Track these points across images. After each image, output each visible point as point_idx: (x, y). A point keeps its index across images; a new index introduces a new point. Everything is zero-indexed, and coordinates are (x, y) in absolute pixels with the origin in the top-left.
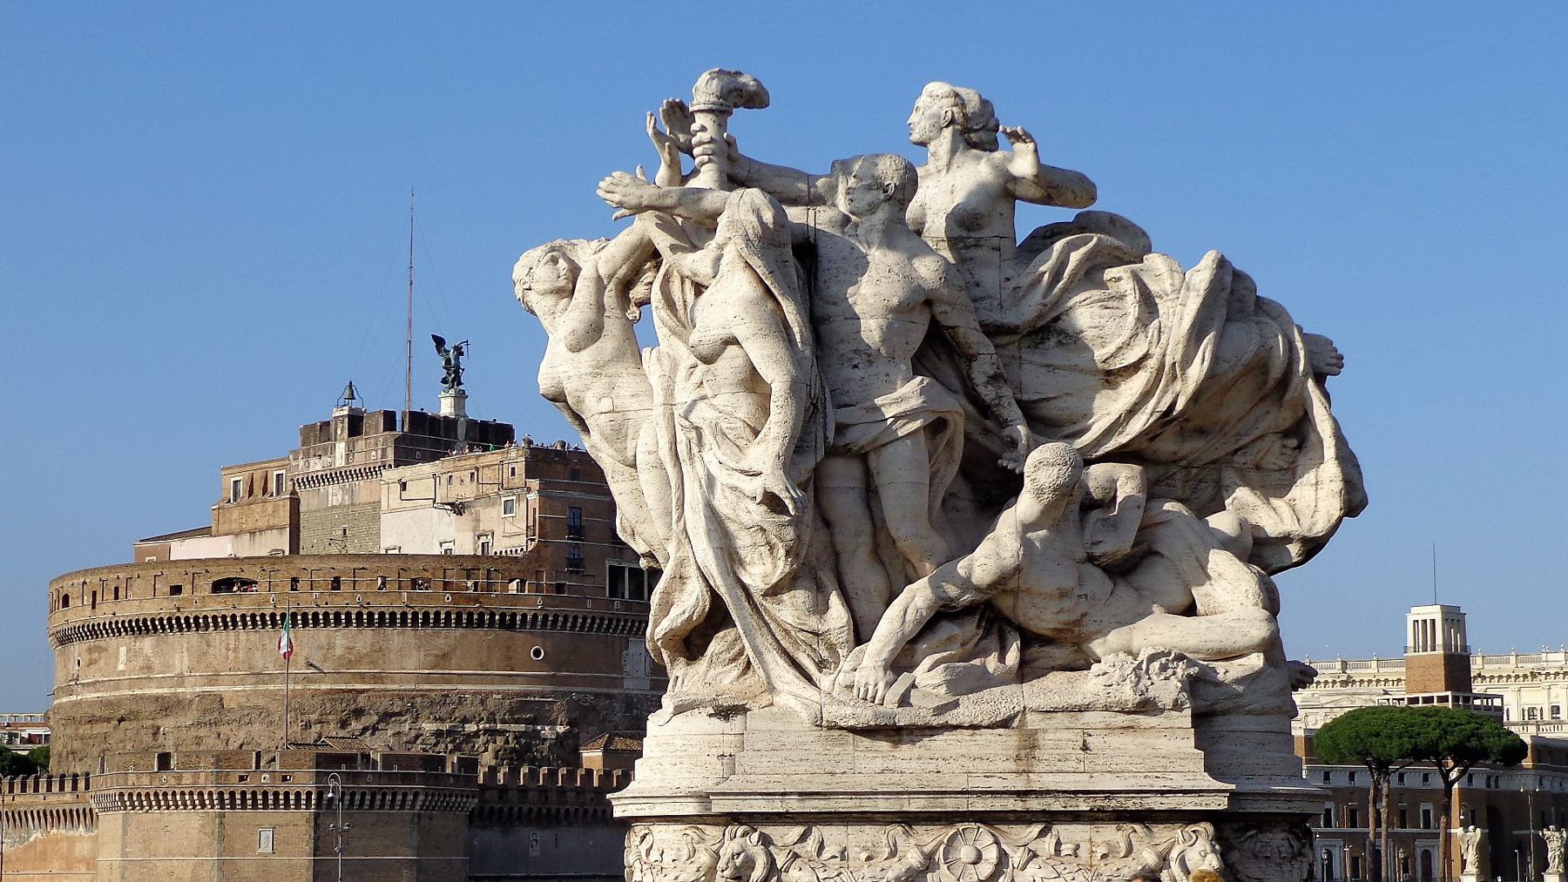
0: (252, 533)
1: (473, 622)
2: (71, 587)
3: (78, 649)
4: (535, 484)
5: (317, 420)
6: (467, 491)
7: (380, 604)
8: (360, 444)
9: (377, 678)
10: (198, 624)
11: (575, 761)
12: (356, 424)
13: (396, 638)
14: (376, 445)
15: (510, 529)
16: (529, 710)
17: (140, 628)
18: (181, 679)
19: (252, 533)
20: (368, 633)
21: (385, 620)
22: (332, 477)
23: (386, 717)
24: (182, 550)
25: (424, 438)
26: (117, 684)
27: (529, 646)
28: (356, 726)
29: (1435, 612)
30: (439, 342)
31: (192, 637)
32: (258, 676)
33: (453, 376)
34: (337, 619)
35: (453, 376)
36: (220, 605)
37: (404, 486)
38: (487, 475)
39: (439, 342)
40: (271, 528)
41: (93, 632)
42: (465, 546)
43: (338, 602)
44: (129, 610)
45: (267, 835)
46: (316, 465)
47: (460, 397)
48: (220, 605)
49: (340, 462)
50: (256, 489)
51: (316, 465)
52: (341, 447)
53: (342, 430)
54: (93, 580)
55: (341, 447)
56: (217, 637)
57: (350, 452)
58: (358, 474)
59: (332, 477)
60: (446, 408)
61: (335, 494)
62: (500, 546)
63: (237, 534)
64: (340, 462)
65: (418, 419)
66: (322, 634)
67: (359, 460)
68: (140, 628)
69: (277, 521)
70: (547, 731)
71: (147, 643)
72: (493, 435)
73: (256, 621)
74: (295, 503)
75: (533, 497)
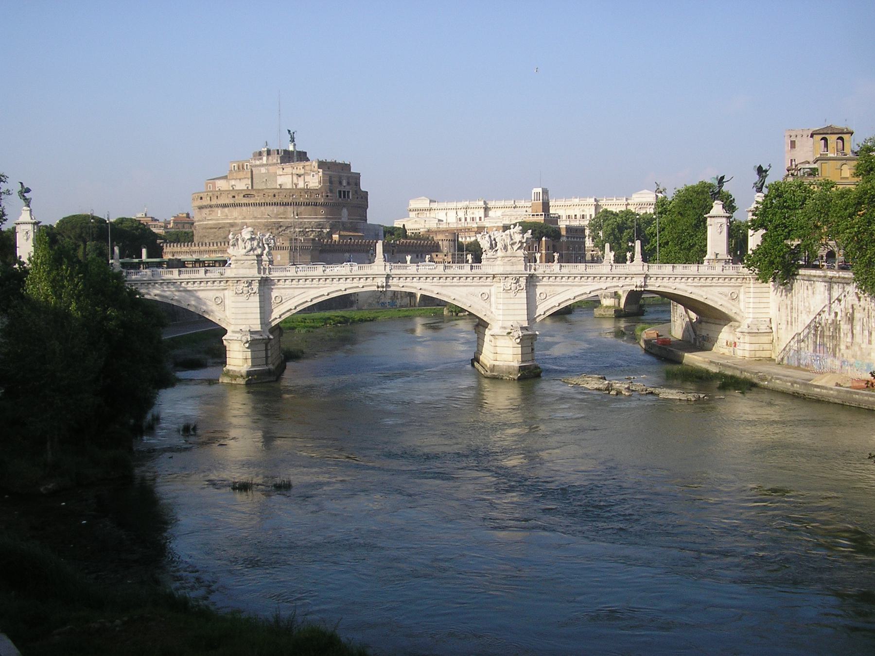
1: (308, 204)
2: (202, 195)
3: (207, 211)
4: (321, 170)
5: (258, 150)
6: (302, 171)
7: (285, 201)
8: (270, 158)
9: (285, 218)
10: (240, 205)
11: (331, 238)
12: (269, 153)
13: (290, 209)
14: (275, 159)
16: (320, 226)
17: (225, 206)
18: (236, 219)
21: (287, 204)
22: (263, 165)
23: (287, 227)
24: (222, 185)
25: (287, 157)
26: (217, 220)
27: (322, 211)
28: (280, 230)
29: (540, 190)
31: (238, 208)
32: (255, 218)
33: (293, 140)
34: (276, 204)
35: (293, 140)
36: (246, 201)
38: (307, 168)
41: (211, 206)
42: (301, 185)
43: (275, 200)
44: (221, 201)
45: (279, 256)
46: (258, 162)
47: (295, 145)
48: (246, 201)
49: (265, 162)
50: (241, 168)
51: (258, 162)
52: (265, 158)
53: (265, 154)
54: (210, 194)
55: (265, 158)
56: (244, 208)
57: (268, 159)
58: (270, 165)
59: (263, 165)
60: (291, 148)
61: (263, 170)
63: (236, 179)
64: (265, 162)
65: (286, 152)
66: (271, 208)
67: (270, 162)
68: (225, 206)
70: (325, 231)
71: (226, 210)
72: (302, 156)
73: (255, 205)
74: (252, 172)
75: (321, 174)
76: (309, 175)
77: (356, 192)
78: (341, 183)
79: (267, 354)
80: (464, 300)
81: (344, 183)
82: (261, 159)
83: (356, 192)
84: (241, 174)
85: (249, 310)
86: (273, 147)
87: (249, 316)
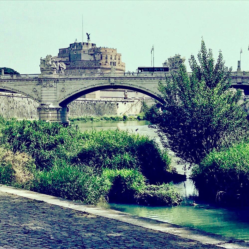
0: (64, 57)
6: (93, 53)
15: (98, 57)
19: (64, 57)
20: (83, 70)
21: (85, 68)
30: (87, 34)
33: (89, 38)
35: (89, 38)
37: (84, 52)
39: (87, 34)
40: (66, 57)
49: (75, 48)
52: (75, 47)
55: (75, 47)
57: (77, 47)
62: (97, 59)
63: (62, 57)
67: (78, 48)
69: (67, 56)
76: (97, 54)
77: (119, 63)
78: (111, 59)
79: (58, 115)
80: (153, 90)
81: (113, 58)
82: (73, 47)
83: (119, 63)
84: (64, 55)
85: (49, 94)
86: (78, 42)
87: (49, 97)
